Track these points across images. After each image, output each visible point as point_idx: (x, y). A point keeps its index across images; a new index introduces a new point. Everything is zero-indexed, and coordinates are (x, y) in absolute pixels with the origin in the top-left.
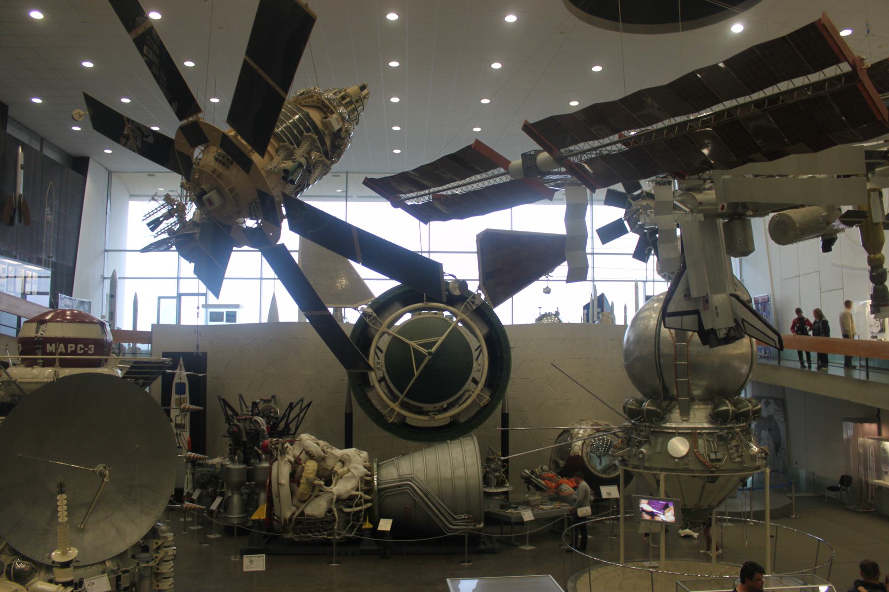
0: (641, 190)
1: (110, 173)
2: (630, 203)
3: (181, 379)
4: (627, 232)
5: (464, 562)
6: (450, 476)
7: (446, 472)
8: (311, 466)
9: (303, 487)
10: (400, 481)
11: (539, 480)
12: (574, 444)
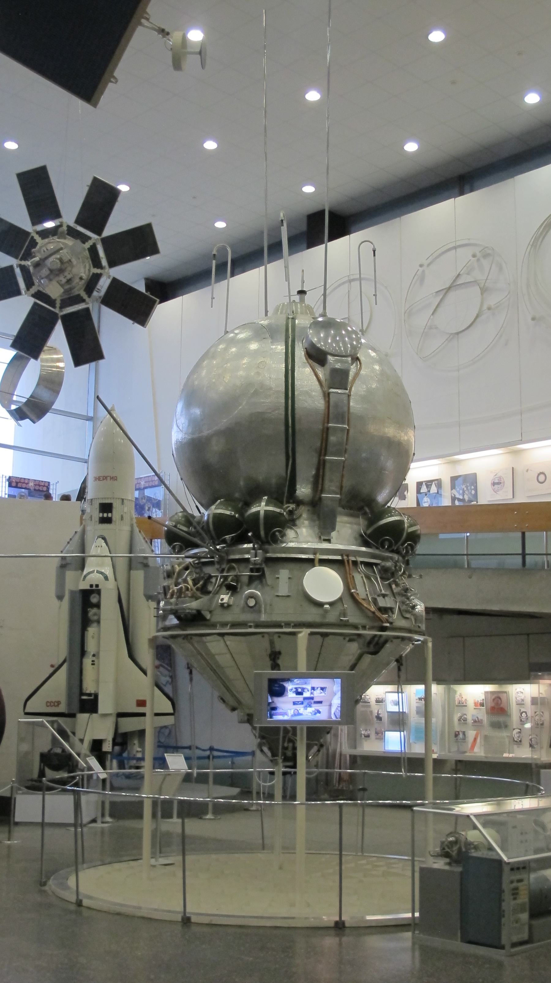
0: (60, 220)
2: (35, 240)
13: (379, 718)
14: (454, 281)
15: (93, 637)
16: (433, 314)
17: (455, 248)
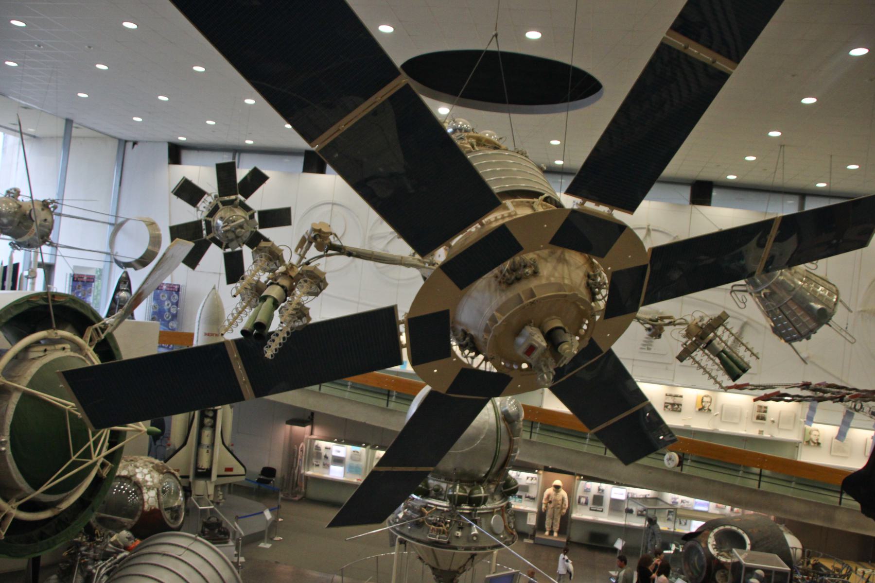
13: (326, 457)
15: (208, 436)
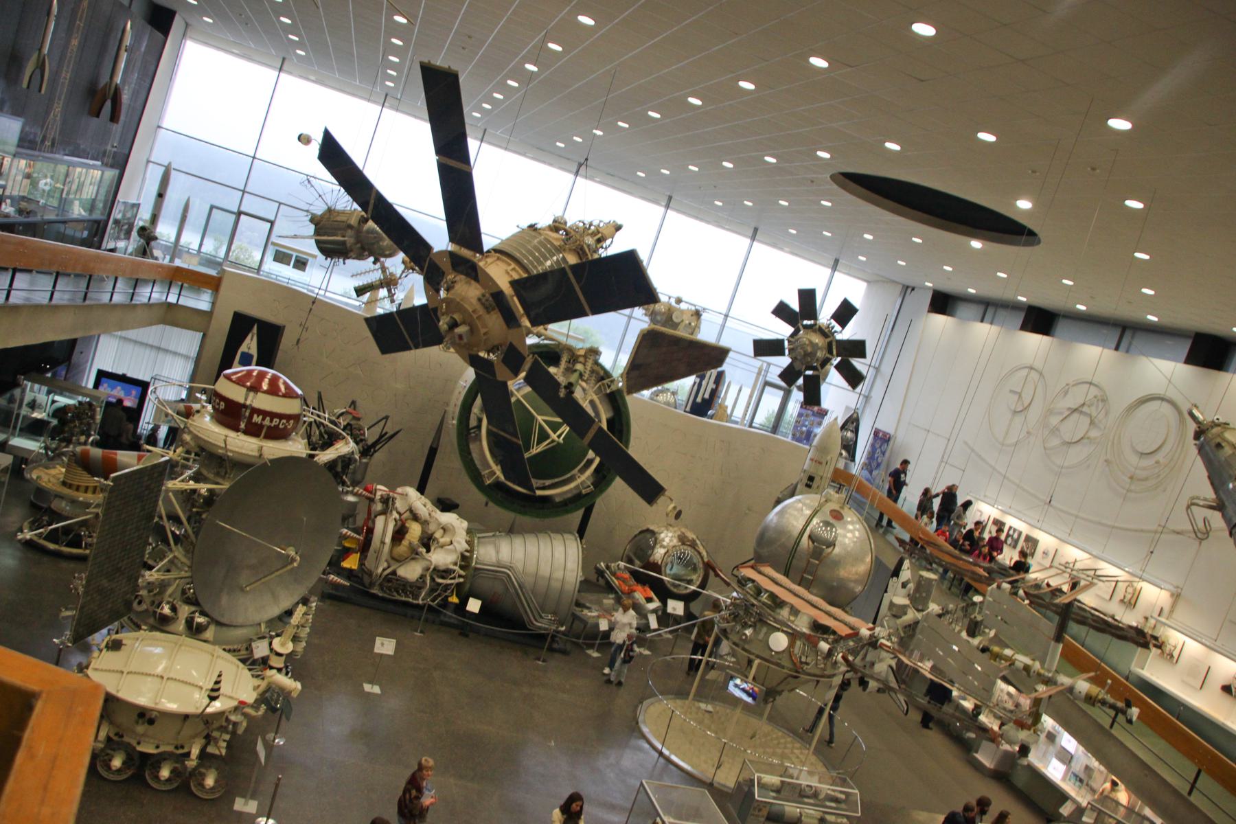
1: (187, 25)
3: (249, 348)
4: (782, 354)
5: (539, 660)
6: (547, 575)
7: (545, 570)
8: (415, 530)
9: (403, 548)
10: (498, 567)
11: (613, 578)
12: (656, 551)
14: (1080, 407)
16: (1062, 420)
17: (1091, 383)
